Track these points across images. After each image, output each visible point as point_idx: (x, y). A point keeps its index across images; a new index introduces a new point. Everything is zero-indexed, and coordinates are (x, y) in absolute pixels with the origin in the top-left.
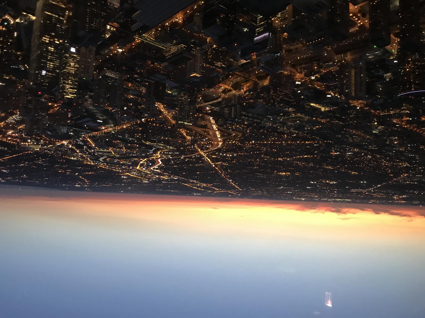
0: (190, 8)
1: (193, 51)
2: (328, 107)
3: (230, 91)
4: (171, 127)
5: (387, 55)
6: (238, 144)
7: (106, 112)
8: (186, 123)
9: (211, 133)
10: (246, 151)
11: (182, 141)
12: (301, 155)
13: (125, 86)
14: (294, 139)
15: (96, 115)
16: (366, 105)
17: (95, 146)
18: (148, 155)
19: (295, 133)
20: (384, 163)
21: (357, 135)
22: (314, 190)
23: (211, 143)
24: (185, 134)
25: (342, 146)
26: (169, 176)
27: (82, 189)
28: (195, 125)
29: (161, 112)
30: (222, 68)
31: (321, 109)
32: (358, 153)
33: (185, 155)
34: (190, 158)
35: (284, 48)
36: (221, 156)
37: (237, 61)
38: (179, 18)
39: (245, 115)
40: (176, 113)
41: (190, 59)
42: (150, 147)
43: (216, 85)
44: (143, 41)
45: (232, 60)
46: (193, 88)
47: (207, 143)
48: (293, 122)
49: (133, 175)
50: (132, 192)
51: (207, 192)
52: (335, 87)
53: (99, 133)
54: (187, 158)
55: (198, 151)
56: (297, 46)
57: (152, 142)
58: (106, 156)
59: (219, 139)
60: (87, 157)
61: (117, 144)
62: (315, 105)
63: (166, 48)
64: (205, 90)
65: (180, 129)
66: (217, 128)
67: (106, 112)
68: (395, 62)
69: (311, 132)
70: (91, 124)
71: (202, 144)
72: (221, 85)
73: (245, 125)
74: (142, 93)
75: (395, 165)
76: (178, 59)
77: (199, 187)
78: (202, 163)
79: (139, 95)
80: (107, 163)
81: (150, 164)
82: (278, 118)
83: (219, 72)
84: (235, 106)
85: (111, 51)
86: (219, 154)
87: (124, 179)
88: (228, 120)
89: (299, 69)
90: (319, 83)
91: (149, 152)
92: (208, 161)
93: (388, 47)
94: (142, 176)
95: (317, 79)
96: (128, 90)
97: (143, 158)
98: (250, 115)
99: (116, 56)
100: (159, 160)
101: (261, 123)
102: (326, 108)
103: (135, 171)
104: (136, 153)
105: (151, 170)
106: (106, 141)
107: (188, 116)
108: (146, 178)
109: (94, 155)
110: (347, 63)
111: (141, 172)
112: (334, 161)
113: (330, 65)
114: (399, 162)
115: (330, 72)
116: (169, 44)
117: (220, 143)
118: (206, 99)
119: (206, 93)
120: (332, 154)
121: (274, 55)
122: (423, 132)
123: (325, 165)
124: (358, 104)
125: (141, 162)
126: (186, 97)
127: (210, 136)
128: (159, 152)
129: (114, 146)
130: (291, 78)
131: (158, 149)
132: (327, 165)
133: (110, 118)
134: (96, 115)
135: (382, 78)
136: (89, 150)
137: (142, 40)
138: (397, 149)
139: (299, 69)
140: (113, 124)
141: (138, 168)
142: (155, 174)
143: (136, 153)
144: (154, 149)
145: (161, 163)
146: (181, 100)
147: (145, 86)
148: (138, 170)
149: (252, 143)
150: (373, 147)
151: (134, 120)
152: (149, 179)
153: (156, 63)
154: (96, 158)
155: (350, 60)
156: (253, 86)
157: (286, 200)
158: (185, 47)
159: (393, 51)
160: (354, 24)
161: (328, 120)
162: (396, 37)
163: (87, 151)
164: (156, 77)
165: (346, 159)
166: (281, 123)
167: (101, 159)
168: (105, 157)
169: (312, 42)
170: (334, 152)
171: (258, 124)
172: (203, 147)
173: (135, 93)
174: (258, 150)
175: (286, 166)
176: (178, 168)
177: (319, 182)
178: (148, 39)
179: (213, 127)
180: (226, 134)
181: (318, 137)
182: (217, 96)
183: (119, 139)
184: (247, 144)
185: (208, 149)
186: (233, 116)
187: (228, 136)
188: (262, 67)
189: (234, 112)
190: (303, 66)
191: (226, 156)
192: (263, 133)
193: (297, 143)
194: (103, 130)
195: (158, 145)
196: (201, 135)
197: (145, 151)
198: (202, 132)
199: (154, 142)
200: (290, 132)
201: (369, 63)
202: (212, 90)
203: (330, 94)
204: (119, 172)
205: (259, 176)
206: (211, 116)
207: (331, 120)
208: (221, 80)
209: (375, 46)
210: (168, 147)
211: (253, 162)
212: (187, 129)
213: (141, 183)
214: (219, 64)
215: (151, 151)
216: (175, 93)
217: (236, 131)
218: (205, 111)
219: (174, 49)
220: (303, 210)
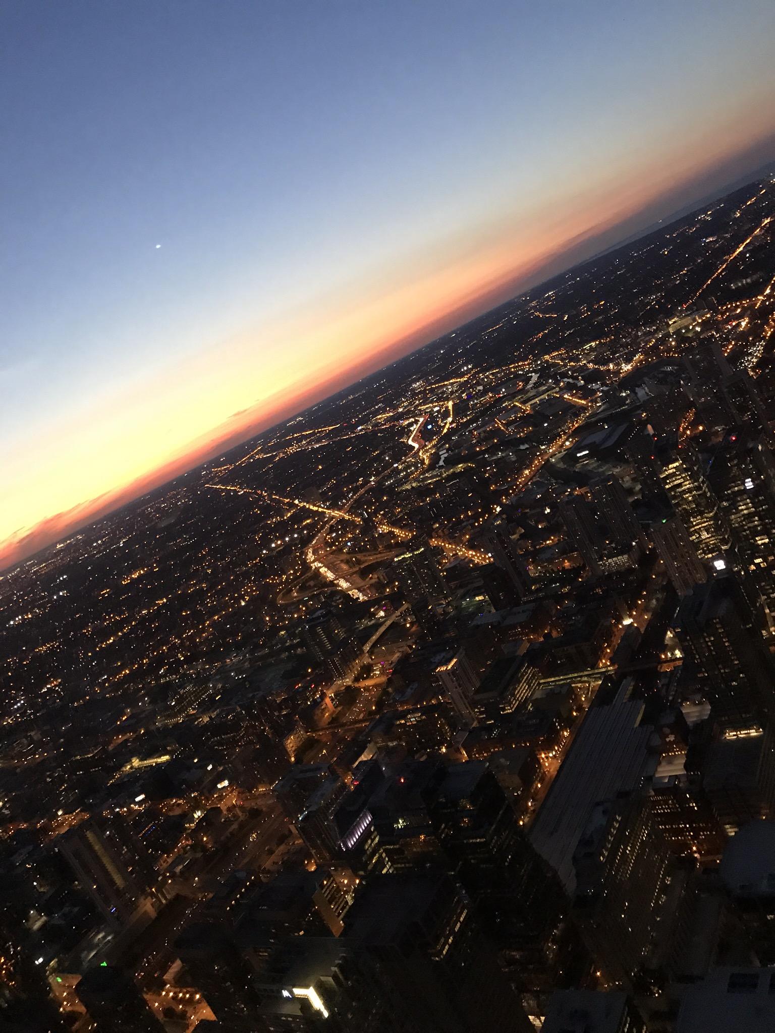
0: (541, 796)
1: (481, 713)
2: (129, 775)
3: (357, 680)
4: (434, 530)
5: (67, 964)
6: (273, 579)
7: (582, 479)
8: (408, 555)
9: (345, 567)
10: (246, 575)
11: (393, 514)
12: (121, 637)
13: (575, 554)
14: (159, 661)
15: (598, 460)
16: (45, 829)
17: (562, 397)
18: (444, 444)
19: (164, 676)
22: (48, 581)
23: (331, 545)
24: (396, 531)
25: (44, 711)
26: (376, 425)
27: (537, 293)
28: (388, 565)
29: (471, 546)
30: (403, 715)
31: (141, 760)
33: (371, 489)
34: (355, 490)
35: (298, 839)
36: (293, 531)
37: (379, 748)
38: (549, 761)
39: (294, 647)
40: (440, 564)
41: (477, 692)
42: (451, 462)
43: (393, 674)
44: (593, 668)
45: (391, 744)
46: (437, 636)
47: (340, 542)
48: (181, 696)
49: (452, 384)
50: (434, 347)
51: (278, 438)
52: (138, 825)
53: (569, 428)
54: (362, 486)
55: (349, 512)
56: (273, 858)
57: (454, 475)
58: (528, 391)
59: (317, 564)
60: (565, 365)
61: (520, 428)
62: (159, 760)
63: (539, 684)
64: (410, 647)
65: (413, 536)
66: (338, 585)
67: (582, 479)
68: (41, 960)
69: (130, 699)
70: (596, 438)
71: (348, 532)
72: (384, 679)
73: (282, 628)
74: (533, 562)
76: (502, 677)
77: (299, 440)
78: (324, 494)
79: (535, 556)
80: (517, 376)
81: (430, 427)
82: (220, 686)
83: (403, 703)
84: (330, 654)
85: (646, 609)
86: (300, 531)
87: (466, 364)
88: (323, 616)
89: (240, 814)
90: (178, 812)
91: (448, 450)
92: (314, 505)
93: (74, 981)
94: (432, 391)
95: (187, 816)
96: (565, 550)
97: (452, 431)
98: (284, 655)
99: (627, 603)
100: (416, 446)
101: (252, 652)
102: (131, 768)
103: (452, 393)
104: (470, 432)
105: (420, 415)
106: (547, 420)
107: (411, 572)
108: (420, 392)
109: (554, 377)
110: (143, 892)
111: (439, 399)
113: (178, 865)
115: (167, 850)
116: (538, 695)
117: (310, 557)
118: (396, 632)
119: (404, 643)
121: (313, 808)
123: (58, 647)
124: (65, 820)
125: (450, 419)
126: (440, 610)
127: (342, 561)
128: (427, 462)
129: (526, 420)
130: (243, 784)
131: (432, 467)
132: (52, 651)
133: (565, 474)
134: (598, 460)
135: (46, 908)
136: (570, 380)
137: (596, 671)
139: (240, 814)
140: (553, 465)
141: (450, 404)
142: (409, 411)
143: (470, 432)
144: (441, 463)
145: (410, 442)
146: (446, 598)
147: (535, 581)
148: (448, 399)
149: (244, 600)
151: (516, 498)
152: (414, 394)
153: (542, 639)
154: (545, 372)
155: (142, 900)
156: (316, 718)
157: (96, 523)
158: (504, 709)
159: (59, 980)
160: (180, 982)
161: (110, 748)
162: (73, 1012)
163: (572, 377)
164: (523, 611)
165: (18, 690)
166: (208, 679)
167: (535, 377)
168: (529, 387)
169: (246, 887)
170: (56, 686)
171: (257, 647)
172: (344, 528)
173: (547, 555)
174: (222, 593)
175: (140, 594)
176: (368, 453)
177: (48, 602)
178: (586, 679)
179: (347, 581)
180: (312, 583)
181: (111, 698)
182: (376, 650)
183: (522, 441)
184: (252, 591)
185: (332, 529)
186: (319, 629)
187: (304, 584)
188: (319, 769)
189: (321, 642)
190: (235, 826)
191: (282, 538)
192: (233, 633)
193: (148, 657)
194: (567, 440)
195: (437, 476)
196: (363, 550)
197: (456, 447)
198: (363, 559)
199: (449, 479)
200: (176, 672)
201: (96, 920)
202: (396, 657)
203: (140, 803)
204: (484, 370)
205: (185, 540)
206: (365, 602)
207: (104, 750)
208: (390, 690)
209: (104, 964)
210: (414, 485)
211: (216, 560)
212: (397, 544)
213: (423, 376)
214: (413, 719)
215: (444, 455)
216: (468, 603)
217: (293, 603)
218: (384, 605)
219: (522, 691)
220: (47, 522)
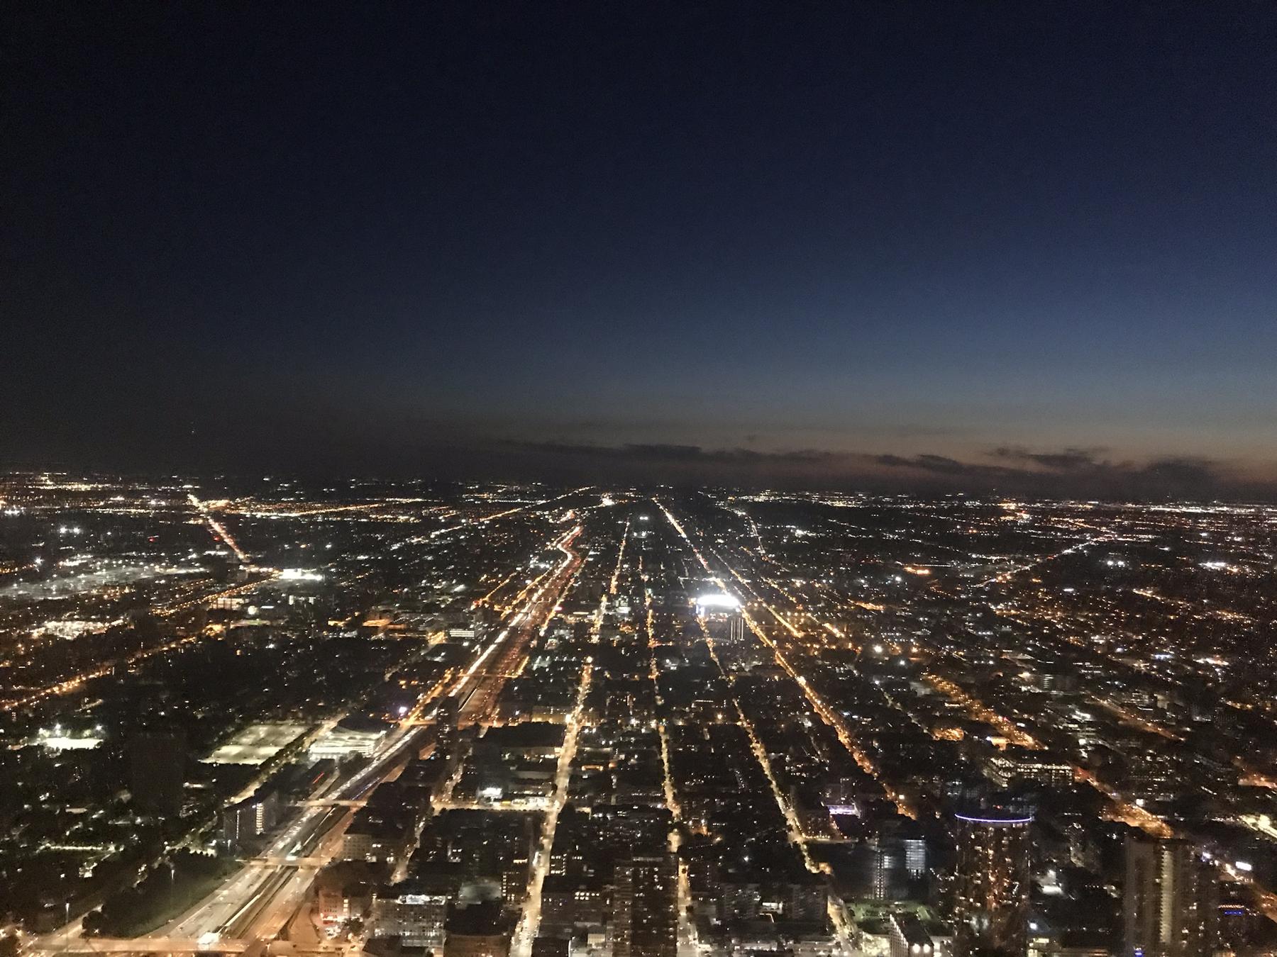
16: (1114, 807)
20: (1055, 616)
21: (1143, 714)
75: (1026, 609)
102: (1254, 825)
112: (1211, 636)
114: (1016, 616)
120: (1223, 659)
122: (956, 695)
124: (1139, 815)
132: (1238, 625)
138: (1020, 656)
150: (1088, 669)
165: (1172, 641)
170: (1218, 666)
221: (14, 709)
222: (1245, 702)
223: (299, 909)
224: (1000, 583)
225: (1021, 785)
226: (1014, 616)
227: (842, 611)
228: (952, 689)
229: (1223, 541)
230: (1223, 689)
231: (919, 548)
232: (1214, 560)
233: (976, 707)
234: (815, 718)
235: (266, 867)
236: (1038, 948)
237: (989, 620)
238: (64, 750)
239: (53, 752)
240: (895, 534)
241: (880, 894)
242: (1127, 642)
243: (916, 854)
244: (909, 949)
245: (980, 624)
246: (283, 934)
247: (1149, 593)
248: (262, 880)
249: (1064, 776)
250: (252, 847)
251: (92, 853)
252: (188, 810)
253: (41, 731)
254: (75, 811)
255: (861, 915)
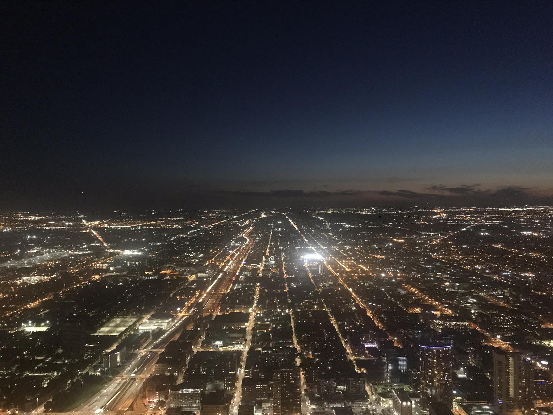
5: (465, 404)
16: (487, 339)
20: (459, 258)
21: (499, 299)
32: (495, 273)
75: (447, 255)
102: (548, 345)
120: (532, 273)
124: (498, 342)
150: (474, 280)
165: (510, 266)
170: (530, 277)
221: (11, 315)
222: (542, 292)
223: (137, 396)
224: (435, 244)
225: (447, 331)
226: (441, 258)
227: (367, 259)
228: (416, 291)
229: (530, 222)
230: (533, 287)
231: (399, 230)
232: (527, 231)
233: (427, 298)
234: (357, 306)
235: (123, 379)
236: (456, 401)
237: (431, 261)
238: (33, 332)
239: (28, 333)
240: (388, 225)
241: (388, 381)
242: (490, 268)
243: (403, 363)
244: (402, 404)
245: (427, 263)
246: (131, 408)
247: (499, 246)
248: (121, 384)
249: (466, 327)
250: (116, 371)
251: (46, 376)
252: (87, 356)
253: (23, 324)
254: (39, 358)
255: (380, 390)
